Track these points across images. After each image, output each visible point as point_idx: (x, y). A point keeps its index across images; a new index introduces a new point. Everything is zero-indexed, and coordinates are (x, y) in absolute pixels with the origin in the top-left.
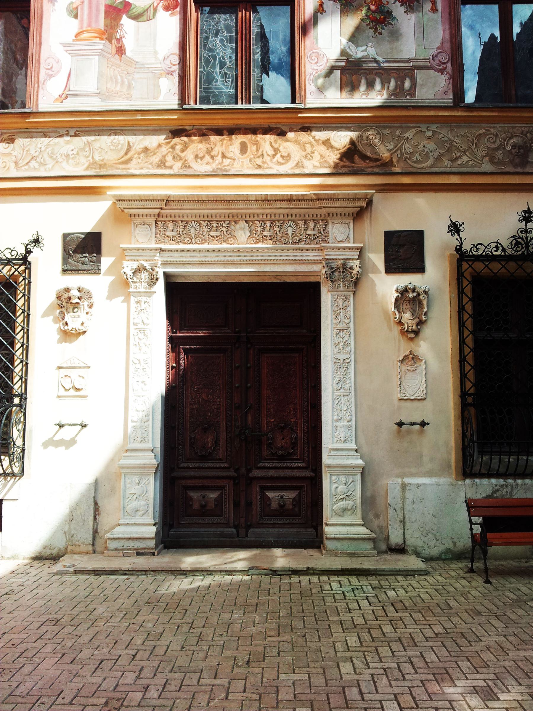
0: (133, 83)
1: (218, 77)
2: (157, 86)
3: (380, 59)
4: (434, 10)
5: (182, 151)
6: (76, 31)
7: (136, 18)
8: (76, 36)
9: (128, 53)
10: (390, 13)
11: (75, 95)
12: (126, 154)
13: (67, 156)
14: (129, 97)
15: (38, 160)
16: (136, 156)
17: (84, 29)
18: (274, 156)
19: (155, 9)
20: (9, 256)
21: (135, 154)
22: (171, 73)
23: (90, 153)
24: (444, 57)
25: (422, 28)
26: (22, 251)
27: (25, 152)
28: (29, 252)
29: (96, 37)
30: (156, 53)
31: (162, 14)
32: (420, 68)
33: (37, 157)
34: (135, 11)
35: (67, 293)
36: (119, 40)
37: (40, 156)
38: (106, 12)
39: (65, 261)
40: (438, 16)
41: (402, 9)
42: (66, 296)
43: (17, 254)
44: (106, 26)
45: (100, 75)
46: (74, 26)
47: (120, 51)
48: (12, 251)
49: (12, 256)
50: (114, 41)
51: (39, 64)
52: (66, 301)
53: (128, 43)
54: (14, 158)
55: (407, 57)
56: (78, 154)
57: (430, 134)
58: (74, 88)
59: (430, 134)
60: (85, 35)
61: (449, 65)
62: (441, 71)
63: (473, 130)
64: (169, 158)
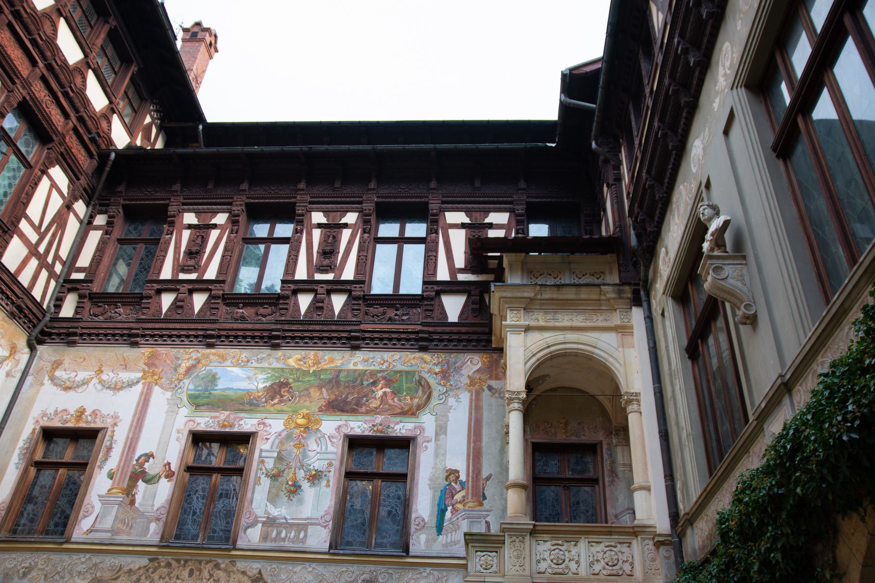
1: (190, 522)
2: (148, 528)
3: (288, 517)
4: (328, 486)
5: (153, 573)
6: (109, 487)
7: (147, 482)
9: (137, 505)
10: (300, 487)
11: (97, 531)
13: (80, 573)
14: (129, 535)
18: (209, 579)
19: (160, 477)
22: (158, 519)
24: (329, 518)
25: (318, 498)
30: (153, 505)
31: (163, 480)
32: (312, 524)
34: (148, 477)
36: (133, 496)
40: (329, 490)
41: (308, 484)
44: (128, 485)
45: (116, 518)
46: (109, 483)
47: (132, 502)
50: (130, 496)
53: (139, 498)
55: (305, 516)
57: (310, 569)
58: (97, 526)
59: (310, 569)
61: (331, 523)
62: (325, 527)
63: (338, 568)
64: (143, 577)
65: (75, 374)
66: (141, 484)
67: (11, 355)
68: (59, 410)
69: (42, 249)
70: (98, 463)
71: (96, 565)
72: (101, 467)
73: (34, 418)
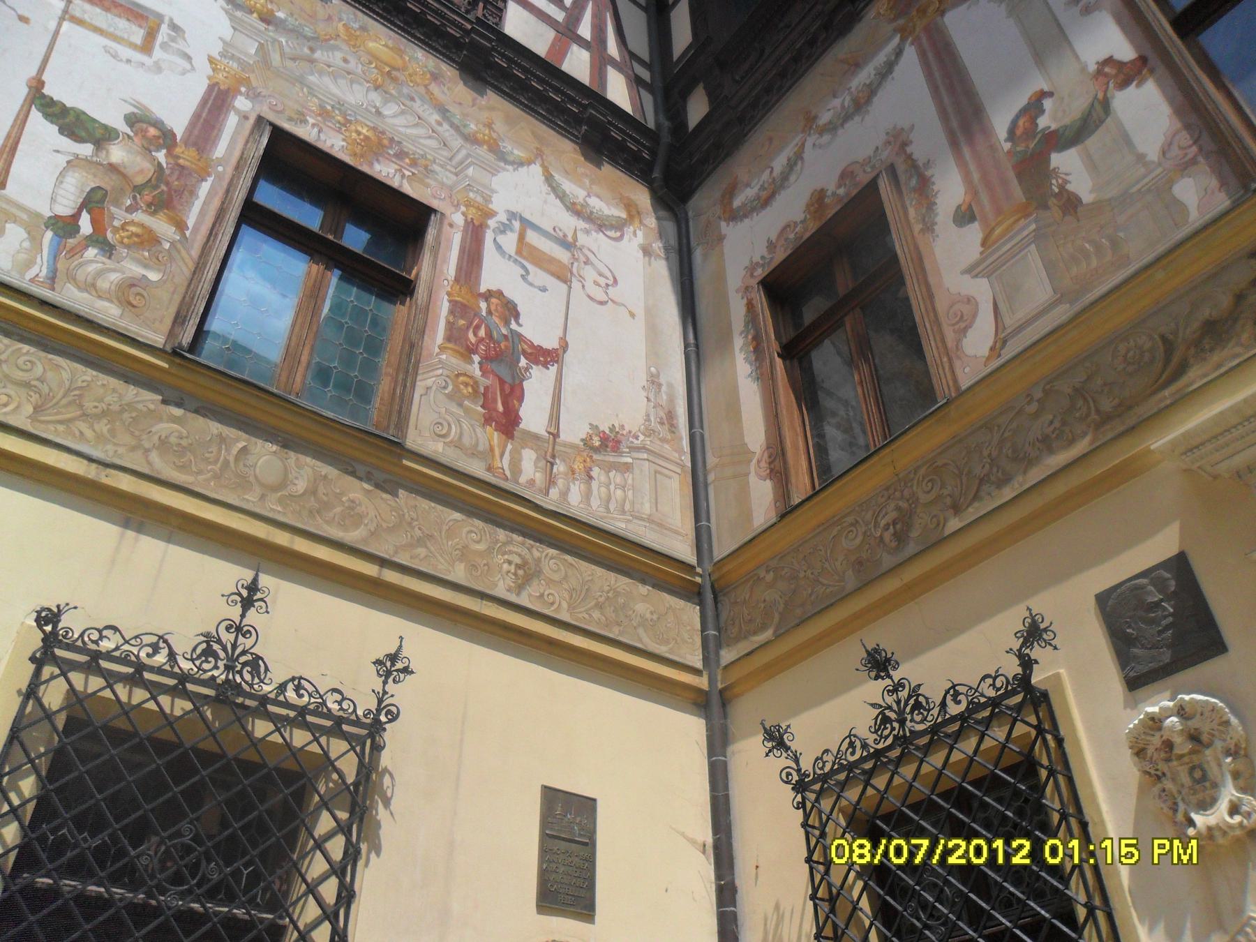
0: (1121, 234)
6: (981, 236)
8: (983, 244)
9: (1087, 197)
11: (1020, 329)
12: (1167, 361)
15: (993, 478)
16: (1192, 351)
17: (993, 224)
20: (991, 693)
21: (1188, 348)
22: (1193, 162)
23: (1089, 408)
26: (1012, 667)
27: (964, 479)
28: (1027, 664)
29: (1018, 220)
30: (1141, 158)
33: (987, 475)
35: (1158, 734)
37: (995, 470)
38: (1019, 176)
39: (1123, 655)
42: (1156, 741)
43: (1008, 682)
45: (1050, 267)
47: (1071, 203)
48: (995, 679)
49: (999, 689)
50: (1052, 202)
51: (939, 325)
52: (1163, 755)
54: (948, 501)
56: (1064, 423)
58: (1010, 321)
60: (998, 231)
65: (768, 171)
66: (1066, 162)
67: (631, 217)
68: (774, 238)
69: (585, 30)
70: (917, 228)
71: (1079, 392)
72: (929, 228)
73: (737, 291)
